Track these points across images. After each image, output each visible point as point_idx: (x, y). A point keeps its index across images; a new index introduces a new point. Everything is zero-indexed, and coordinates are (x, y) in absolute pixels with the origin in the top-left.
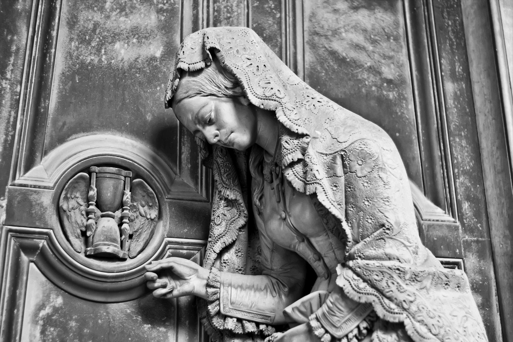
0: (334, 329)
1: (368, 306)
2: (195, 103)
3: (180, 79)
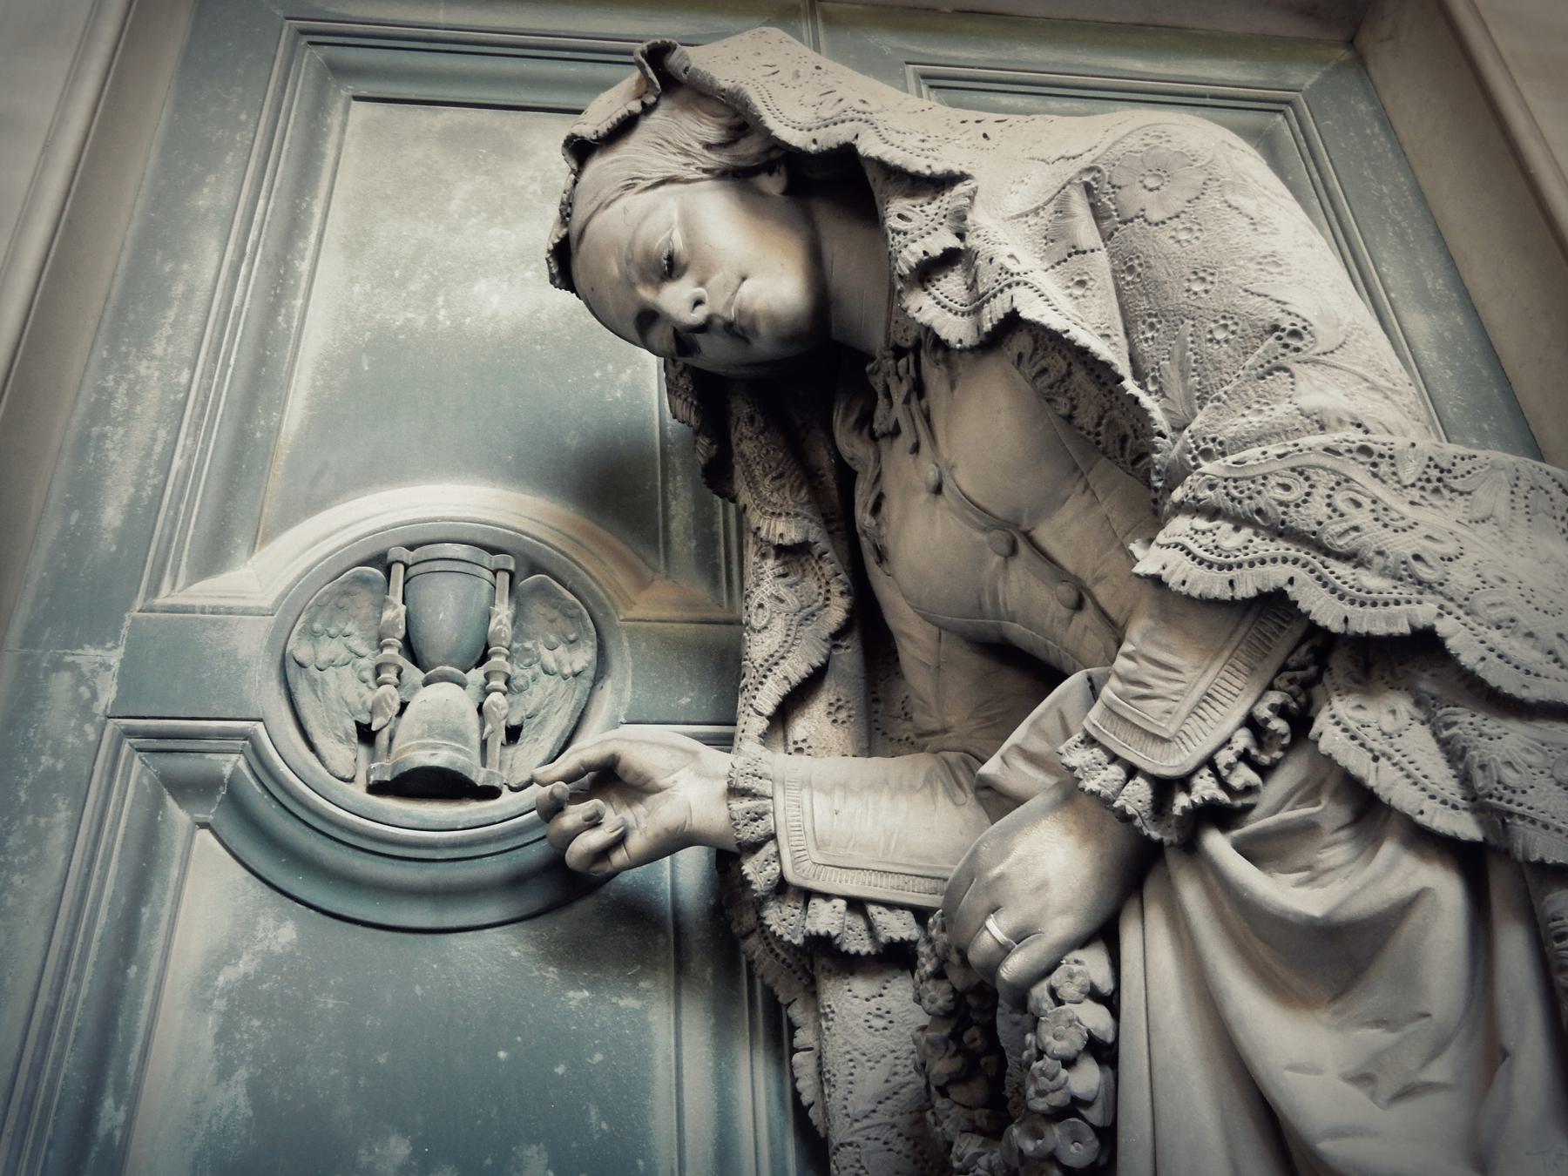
0: (1156, 749)
1: (1274, 605)
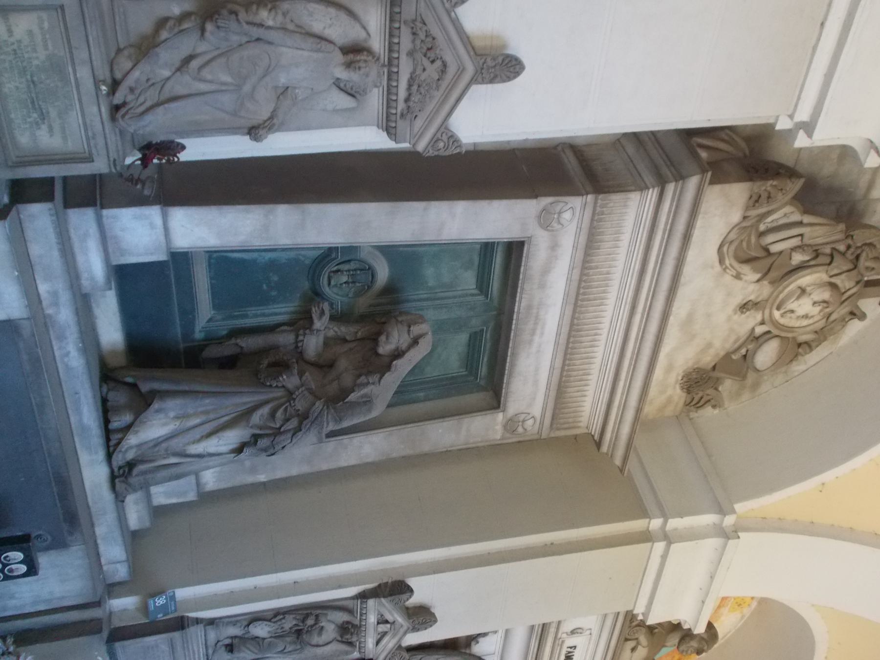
2: (395, 334)
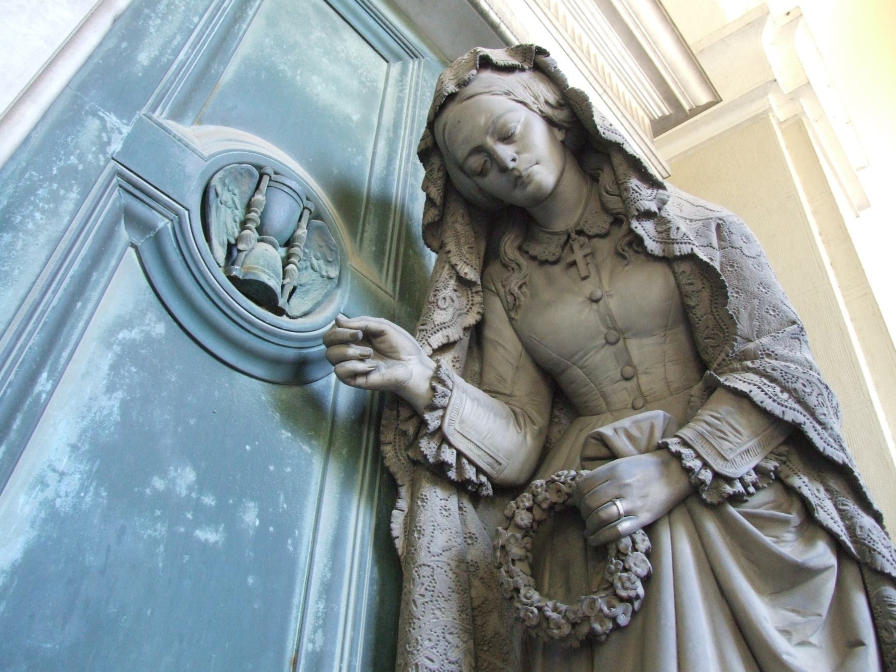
3: (478, 71)
